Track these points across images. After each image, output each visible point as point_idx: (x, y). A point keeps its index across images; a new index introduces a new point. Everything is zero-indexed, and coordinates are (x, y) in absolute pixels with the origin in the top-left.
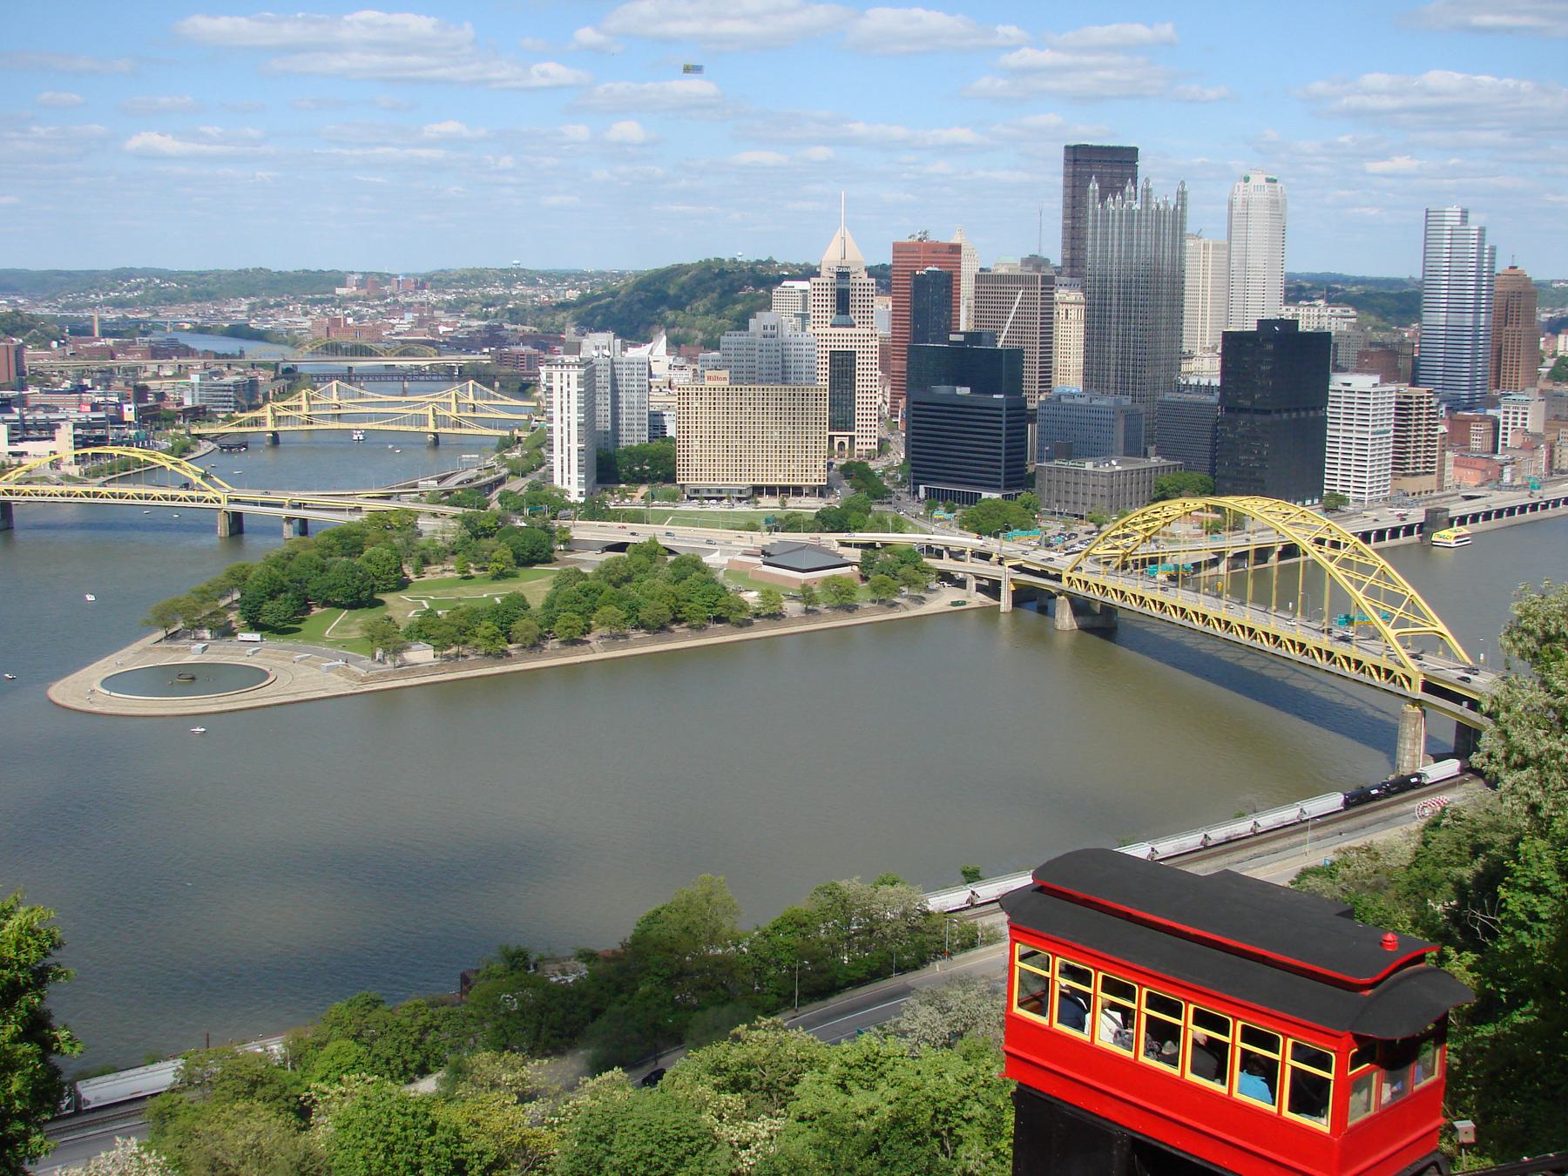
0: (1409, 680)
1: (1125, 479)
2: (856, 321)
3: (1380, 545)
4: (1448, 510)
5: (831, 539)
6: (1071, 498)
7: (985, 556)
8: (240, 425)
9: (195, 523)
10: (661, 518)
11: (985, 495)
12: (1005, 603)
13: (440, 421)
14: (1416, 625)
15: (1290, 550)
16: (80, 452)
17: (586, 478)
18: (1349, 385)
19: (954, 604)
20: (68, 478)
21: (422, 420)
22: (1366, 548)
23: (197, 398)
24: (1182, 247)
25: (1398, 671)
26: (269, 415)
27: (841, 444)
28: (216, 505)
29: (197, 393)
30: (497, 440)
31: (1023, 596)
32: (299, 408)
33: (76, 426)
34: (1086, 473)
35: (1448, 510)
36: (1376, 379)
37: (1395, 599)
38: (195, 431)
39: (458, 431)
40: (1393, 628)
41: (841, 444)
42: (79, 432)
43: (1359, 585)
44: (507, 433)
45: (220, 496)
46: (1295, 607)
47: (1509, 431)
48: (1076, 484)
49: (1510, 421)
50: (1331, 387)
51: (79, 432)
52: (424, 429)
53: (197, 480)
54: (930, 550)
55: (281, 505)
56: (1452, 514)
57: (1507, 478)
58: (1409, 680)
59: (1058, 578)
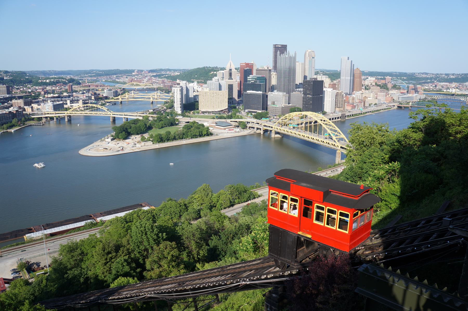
0: (338, 146)
2: (233, 78)
5: (229, 121)
7: (258, 124)
8: (114, 100)
9: (106, 118)
10: (196, 117)
11: (258, 111)
12: (262, 132)
13: (154, 98)
14: (339, 136)
15: (316, 122)
16: (84, 105)
17: (182, 109)
20: (82, 110)
21: (150, 98)
22: (329, 121)
23: (106, 94)
24: (295, 64)
25: (336, 145)
26: (120, 98)
27: (231, 102)
28: (110, 115)
29: (106, 93)
30: (164, 102)
31: (266, 131)
32: (126, 96)
33: (83, 100)
36: (332, 89)
37: (336, 131)
38: (106, 101)
39: (157, 100)
41: (231, 102)
42: (83, 101)
43: (329, 128)
44: (166, 101)
45: (111, 114)
49: (357, 97)
51: (83, 101)
52: (150, 100)
53: (106, 110)
54: (248, 122)
55: (122, 115)
57: (356, 108)
58: (338, 146)
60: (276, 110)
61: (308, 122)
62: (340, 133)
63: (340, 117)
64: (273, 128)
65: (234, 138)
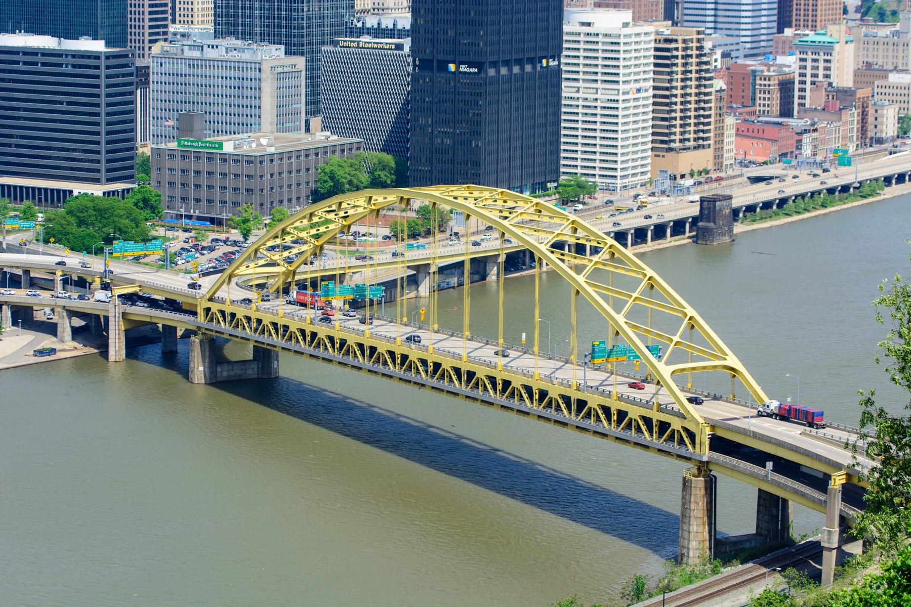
1: (281, 166)
3: (642, 248)
4: (730, 198)
6: (204, 194)
11: (78, 188)
18: (589, 24)
19: (40, 353)
25: (676, 424)
34: (224, 158)
35: (730, 198)
40: (668, 363)
46: (530, 339)
47: (808, 86)
48: (209, 173)
49: (809, 72)
50: (566, 28)
56: (736, 203)
57: (807, 150)
58: (692, 436)
60: (217, 181)
61: (461, 264)
62: (705, 341)
63: (695, 220)
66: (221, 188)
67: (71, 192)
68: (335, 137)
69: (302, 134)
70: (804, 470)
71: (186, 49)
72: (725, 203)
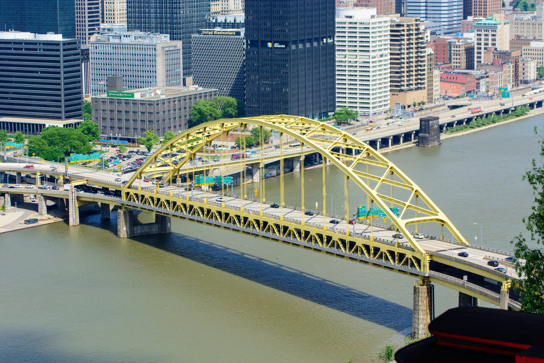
1: (169, 106)
3: (386, 150)
6: (124, 124)
11: (48, 123)
18: (351, 17)
19: (28, 222)
25: (409, 255)
34: (135, 103)
40: (403, 218)
46: (321, 207)
47: (483, 51)
48: (126, 112)
49: (483, 42)
50: (337, 20)
56: (441, 122)
57: (483, 89)
58: (418, 261)
59: (117, 193)
60: (131, 116)
61: (278, 162)
62: (425, 205)
63: (417, 132)
64: (123, 195)
65: (48, 225)
66: (134, 120)
67: (44, 125)
68: (201, 88)
69: (181, 87)
70: (486, 280)
71: (111, 38)
72: (435, 122)
